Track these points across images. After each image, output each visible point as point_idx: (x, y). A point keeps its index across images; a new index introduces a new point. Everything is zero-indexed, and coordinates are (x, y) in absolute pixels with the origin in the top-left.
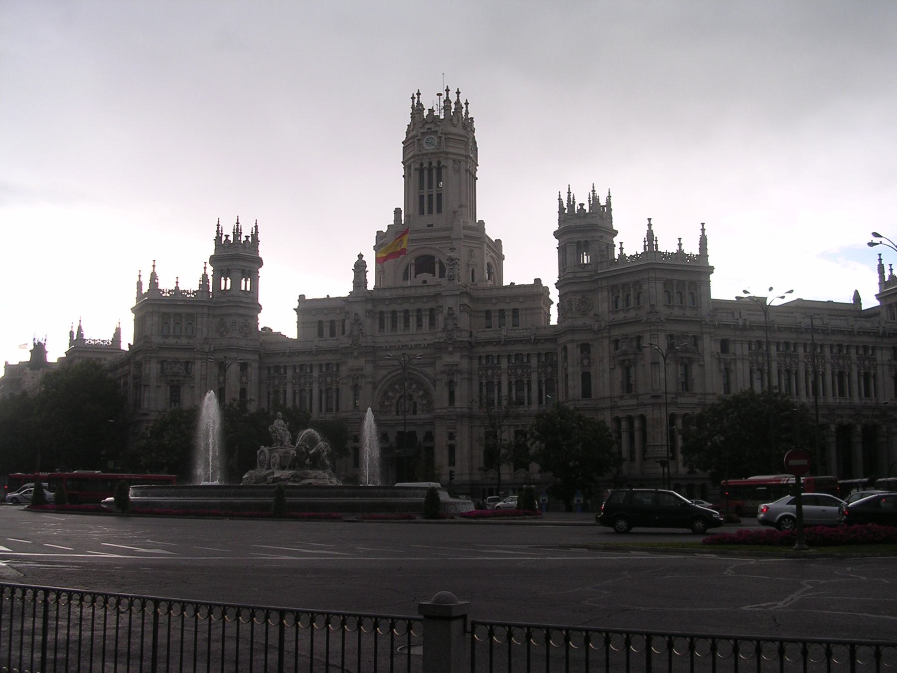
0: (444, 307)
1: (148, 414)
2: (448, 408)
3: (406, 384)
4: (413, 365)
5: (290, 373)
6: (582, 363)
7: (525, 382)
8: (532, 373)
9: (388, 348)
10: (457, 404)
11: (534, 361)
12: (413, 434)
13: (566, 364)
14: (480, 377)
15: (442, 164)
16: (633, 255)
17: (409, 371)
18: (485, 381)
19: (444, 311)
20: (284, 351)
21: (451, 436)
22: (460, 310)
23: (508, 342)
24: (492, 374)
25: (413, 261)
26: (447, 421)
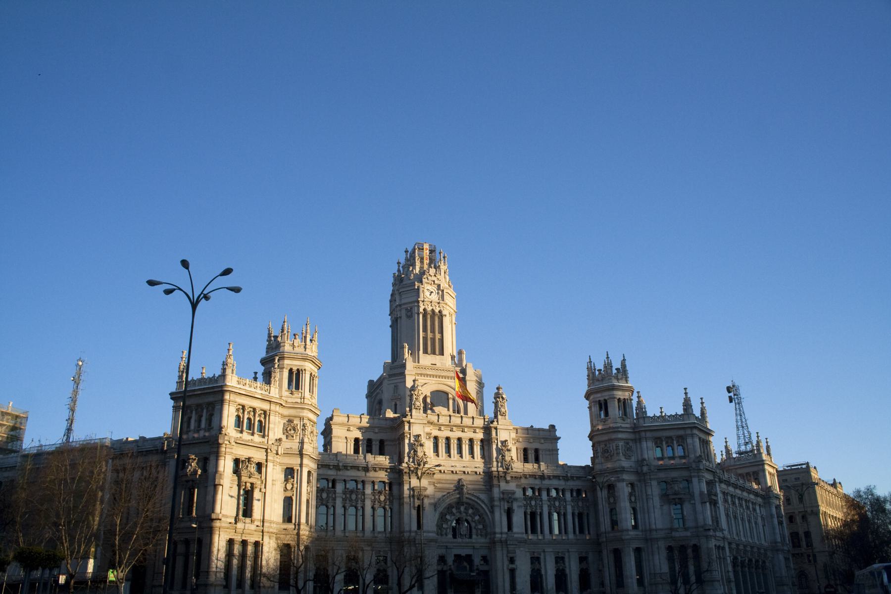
1: (220, 520)
3: (462, 509)
5: (340, 487)
6: (631, 500)
7: (562, 513)
10: (515, 530)
12: (469, 558)
13: (612, 500)
14: (525, 506)
15: (444, 313)
16: (673, 414)
17: (467, 496)
20: (336, 464)
21: (512, 560)
23: (549, 477)
25: (429, 394)
26: (509, 546)
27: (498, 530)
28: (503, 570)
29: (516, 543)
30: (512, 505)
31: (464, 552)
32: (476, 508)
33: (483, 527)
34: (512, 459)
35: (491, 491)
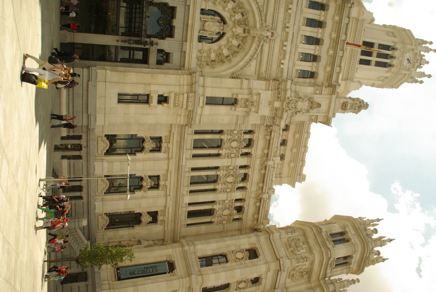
0: (320, 96)
2: (204, 95)
3: (239, 30)
4: (262, 45)
6: (241, 282)
8: (226, 194)
9: (290, 11)
10: (208, 108)
11: (239, 195)
13: (240, 255)
17: (256, 39)
18: (225, 139)
19: (316, 96)
21: (163, 100)
22: (312, 116)
24: (233, 148)
26: (186, 95)
27: (209, 81)
28: (150, 84)
29: (190, 108)
30: (241, 107)
31: (177, 23)
32: (238, 52)
33: (212, 61)
34: (296, 113)
35: (258, 79)
